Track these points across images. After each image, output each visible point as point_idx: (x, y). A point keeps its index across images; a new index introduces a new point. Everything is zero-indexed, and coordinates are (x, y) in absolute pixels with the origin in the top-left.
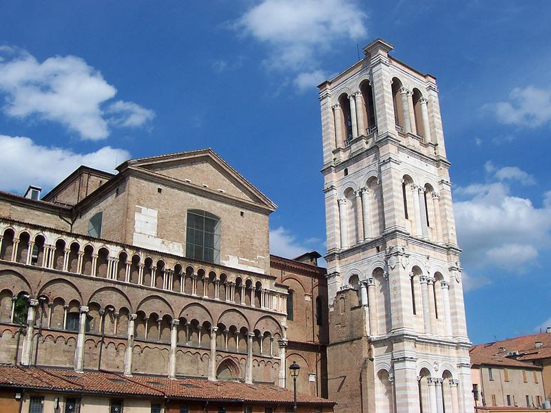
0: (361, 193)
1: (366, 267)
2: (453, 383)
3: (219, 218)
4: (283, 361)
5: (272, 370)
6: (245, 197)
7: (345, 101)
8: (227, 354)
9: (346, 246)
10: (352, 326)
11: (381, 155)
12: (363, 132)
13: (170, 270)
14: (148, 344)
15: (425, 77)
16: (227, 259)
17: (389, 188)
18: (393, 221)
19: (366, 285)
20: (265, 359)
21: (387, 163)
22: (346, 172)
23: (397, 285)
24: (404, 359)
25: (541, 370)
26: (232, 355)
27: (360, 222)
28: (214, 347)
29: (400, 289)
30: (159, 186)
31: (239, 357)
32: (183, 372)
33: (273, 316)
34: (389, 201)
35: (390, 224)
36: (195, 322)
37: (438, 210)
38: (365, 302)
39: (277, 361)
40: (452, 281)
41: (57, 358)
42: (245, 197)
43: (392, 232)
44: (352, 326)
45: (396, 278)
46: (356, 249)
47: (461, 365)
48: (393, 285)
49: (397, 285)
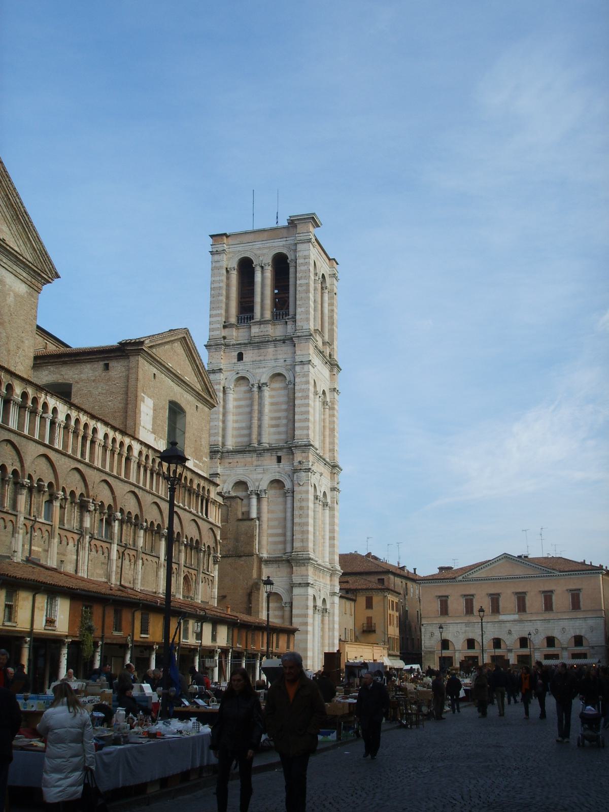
0: (259, 388)
1: (260, 476)
2: (326, 612)
4: (216, 579)
7: (246, 268)
9: (230, 444)
10: (237, 540)
11: (298, 352)
12: (268, 315)
15: (330, 259)
17: (304, 394)
18: (305, 432)
19: (258, 495)
21: (304, 364)
22: (240, 357)
23: (304, 504)
24: (308, 584)
25: (354, 601)
27: (255, 422)
28: (182, 562)
29: (308, 509)
30: (155, 371)
34: (303, 409)
35: (300, 435)
37: (327, 421)
38: (254, 515)
40: (333, 502)
43: (305, 446)
44: (237, 540)
45: (304, 496)
46: (245, 450)
47: (333, 594)
48: (298, 504)
49: (304, 504)
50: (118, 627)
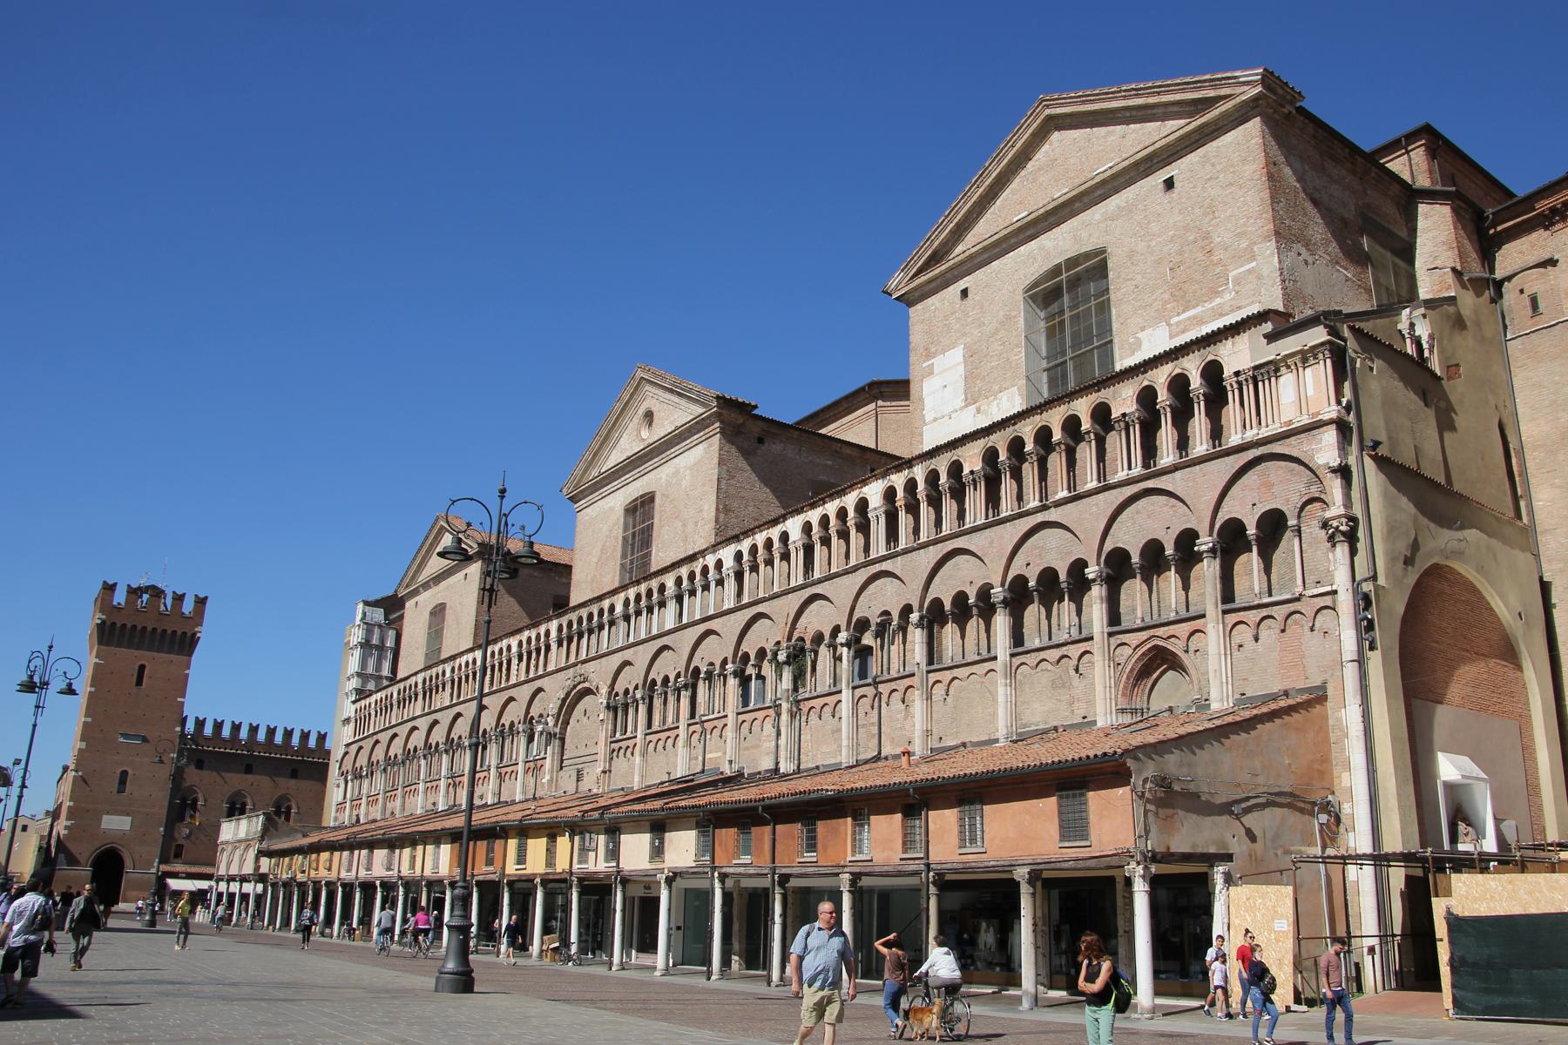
3: (1101, 252)
5: (1312, 642)
6: (1174, 127)
8: (1144, 635)
13: (972, 472)
14: (956, 672)
16: (1138, 345)
20: (1274, 611)
26: (1161, 631)
31: (1183, 629)
32: (1035, 720)
33: (1277, 448)
36: (1048, 576)
39: (1327, 601)
41: (825, 749)
42: (1174, 127)
50: (490, 862)
